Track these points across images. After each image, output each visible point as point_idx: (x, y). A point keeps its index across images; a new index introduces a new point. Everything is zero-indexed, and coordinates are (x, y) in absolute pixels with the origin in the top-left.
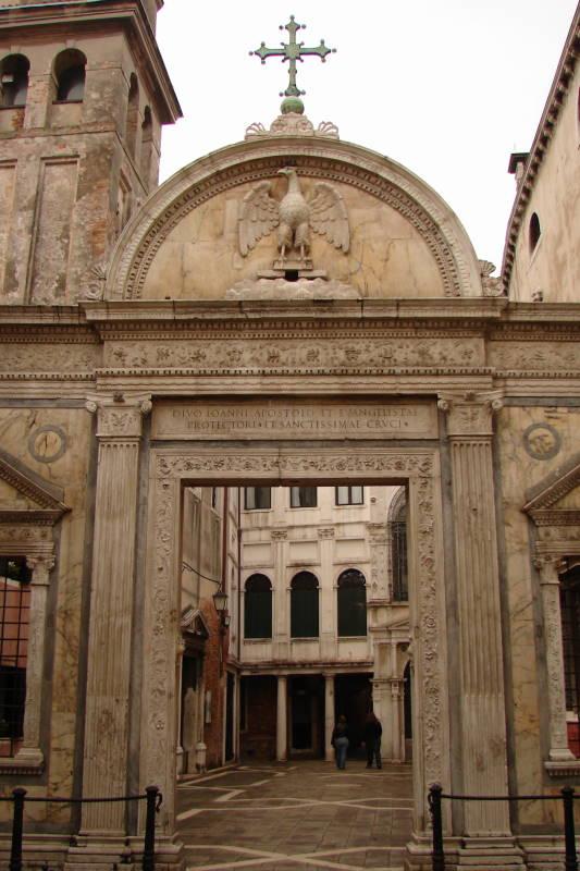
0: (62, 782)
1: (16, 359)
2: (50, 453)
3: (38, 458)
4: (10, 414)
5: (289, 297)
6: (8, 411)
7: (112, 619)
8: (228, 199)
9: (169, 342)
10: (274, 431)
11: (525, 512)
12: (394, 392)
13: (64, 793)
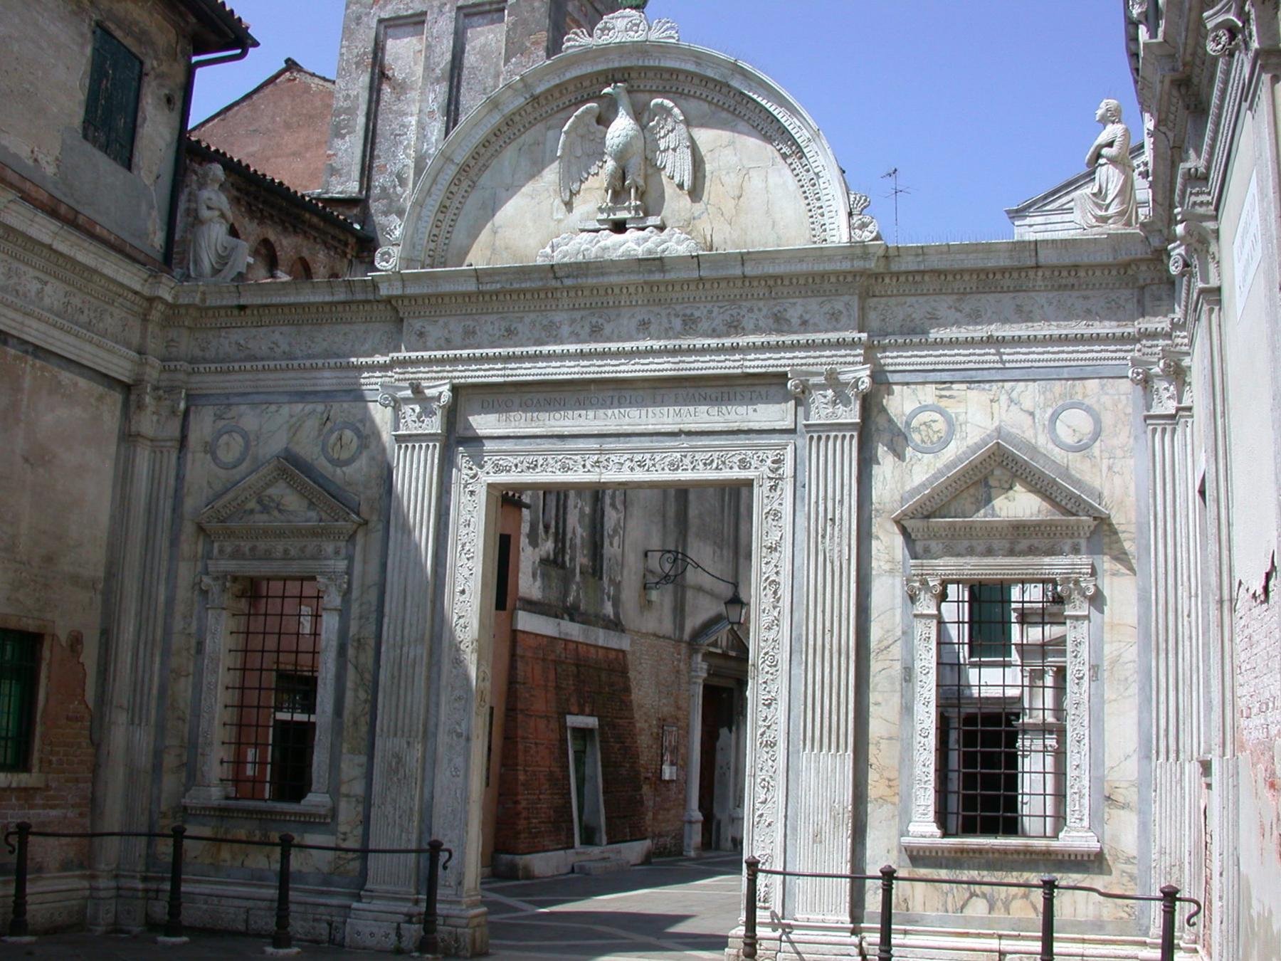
0: (351, 832)
1: (309, 343)
2: (345, 455)
3: (331, 461)
4: (303, 409)
5: (615, 255)
6: (300, 406)
7: (405, 649)
8: (548, 129)
9: (476, 317)
10: (597, 422)
11: (898, 522)
12: (739, 371)
13: (352, 843)
